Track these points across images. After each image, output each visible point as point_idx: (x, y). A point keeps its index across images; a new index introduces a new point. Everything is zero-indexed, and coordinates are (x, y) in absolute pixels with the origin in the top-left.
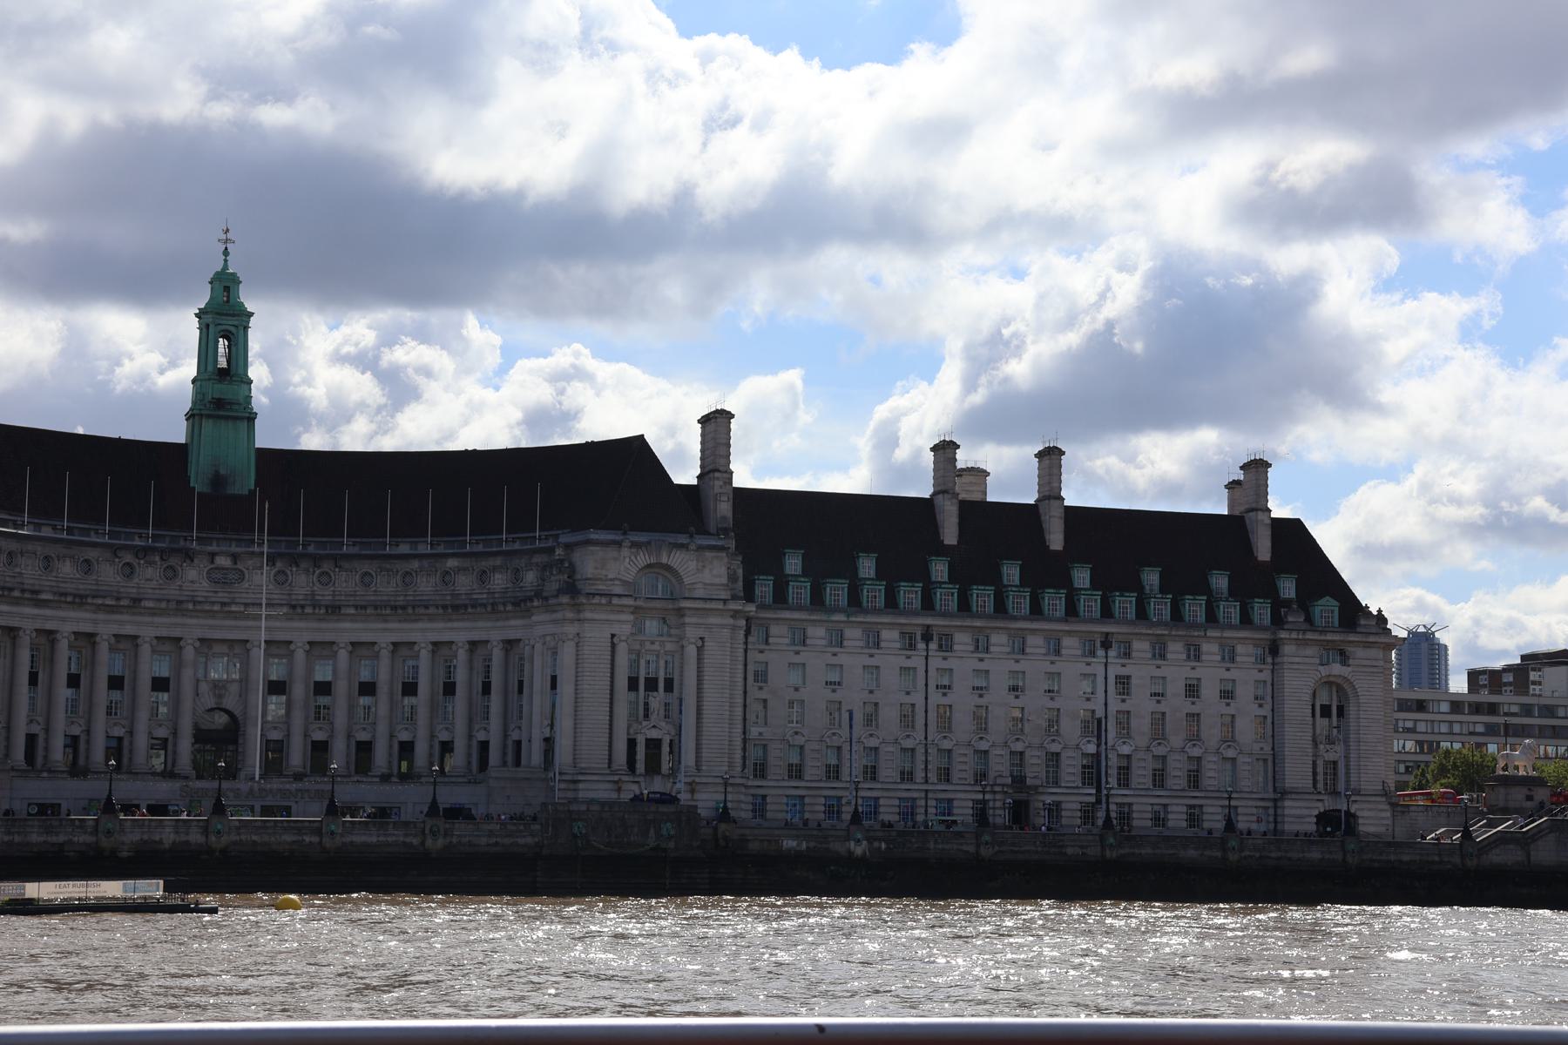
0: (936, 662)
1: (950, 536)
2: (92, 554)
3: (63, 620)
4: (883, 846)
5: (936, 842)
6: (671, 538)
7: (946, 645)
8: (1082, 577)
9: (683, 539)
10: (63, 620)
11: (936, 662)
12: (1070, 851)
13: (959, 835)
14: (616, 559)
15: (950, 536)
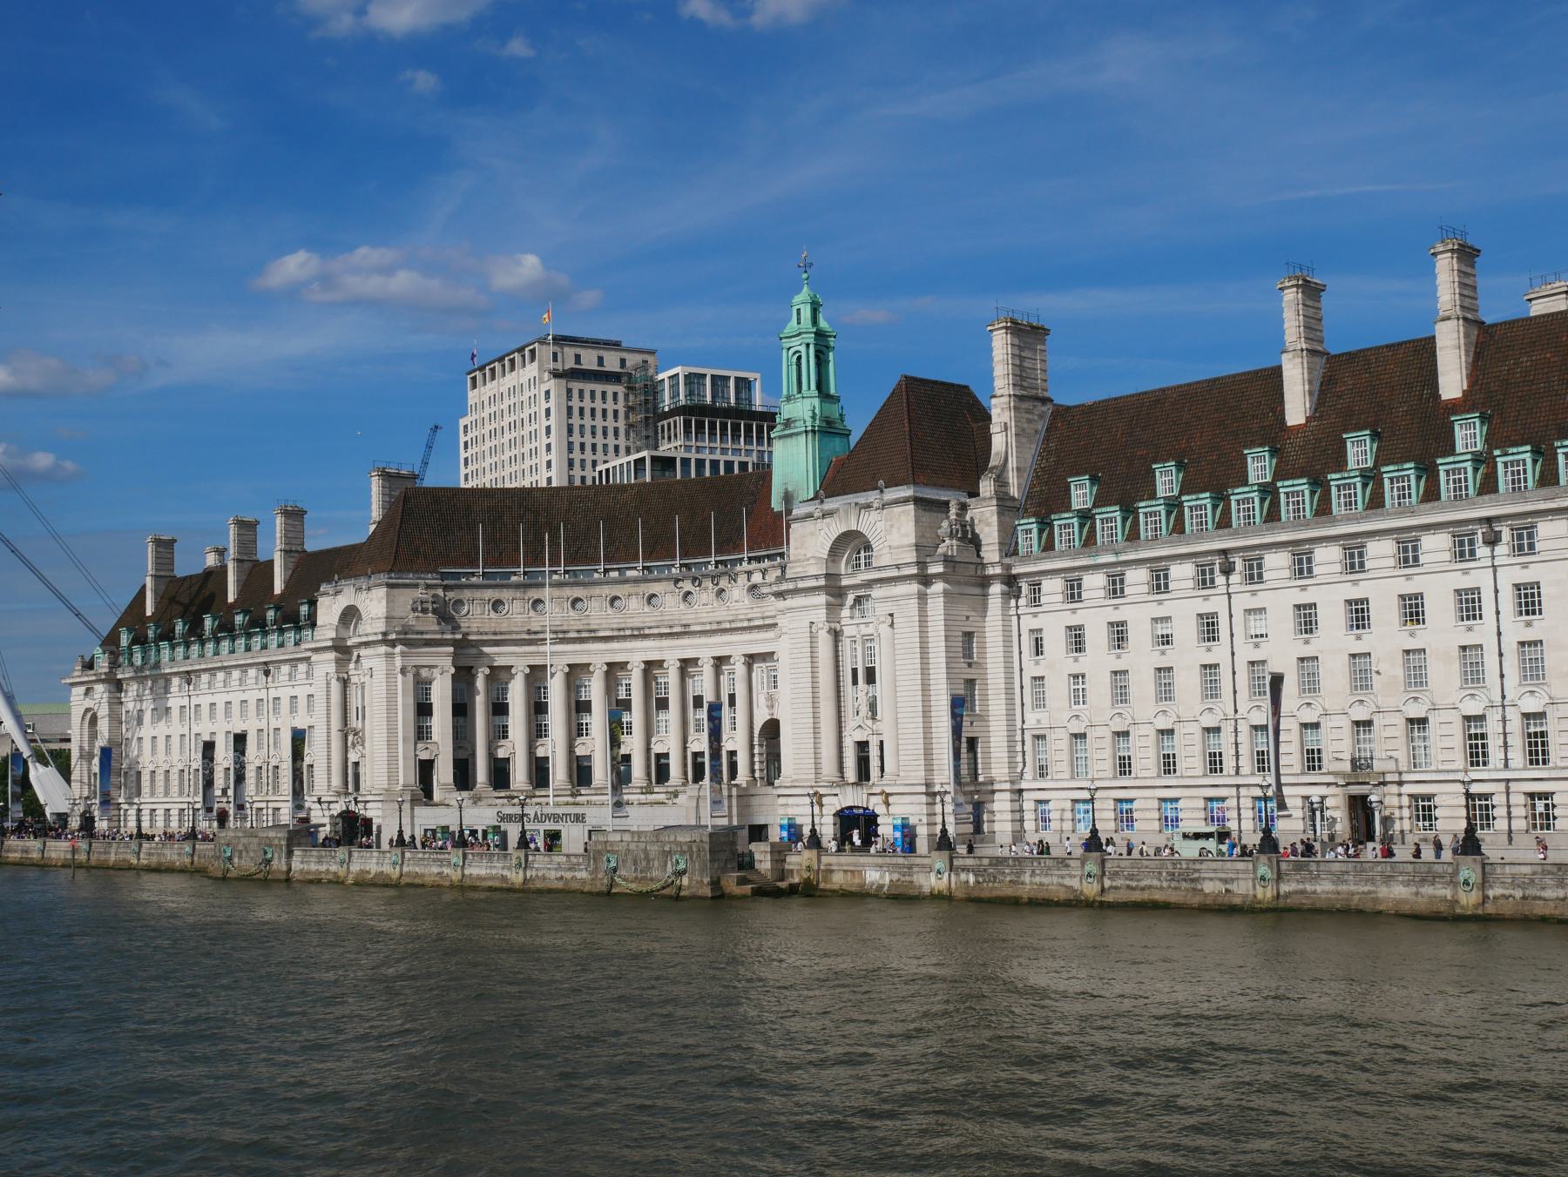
0: (1242, 601)
1: (1296, 410)
2: (655, 588)
3: (631, 650)
4: (972, 879)
5: (1033, 873)
6: (862, 498)
7: (1254, 575)
8: (1468, 435)
9: (872, 497)
10: (631, 650)
11: (1242, 601)
12: (1208, 887)
13: (1063, 862)
14: (812, 534)
15: (1296, 410)
